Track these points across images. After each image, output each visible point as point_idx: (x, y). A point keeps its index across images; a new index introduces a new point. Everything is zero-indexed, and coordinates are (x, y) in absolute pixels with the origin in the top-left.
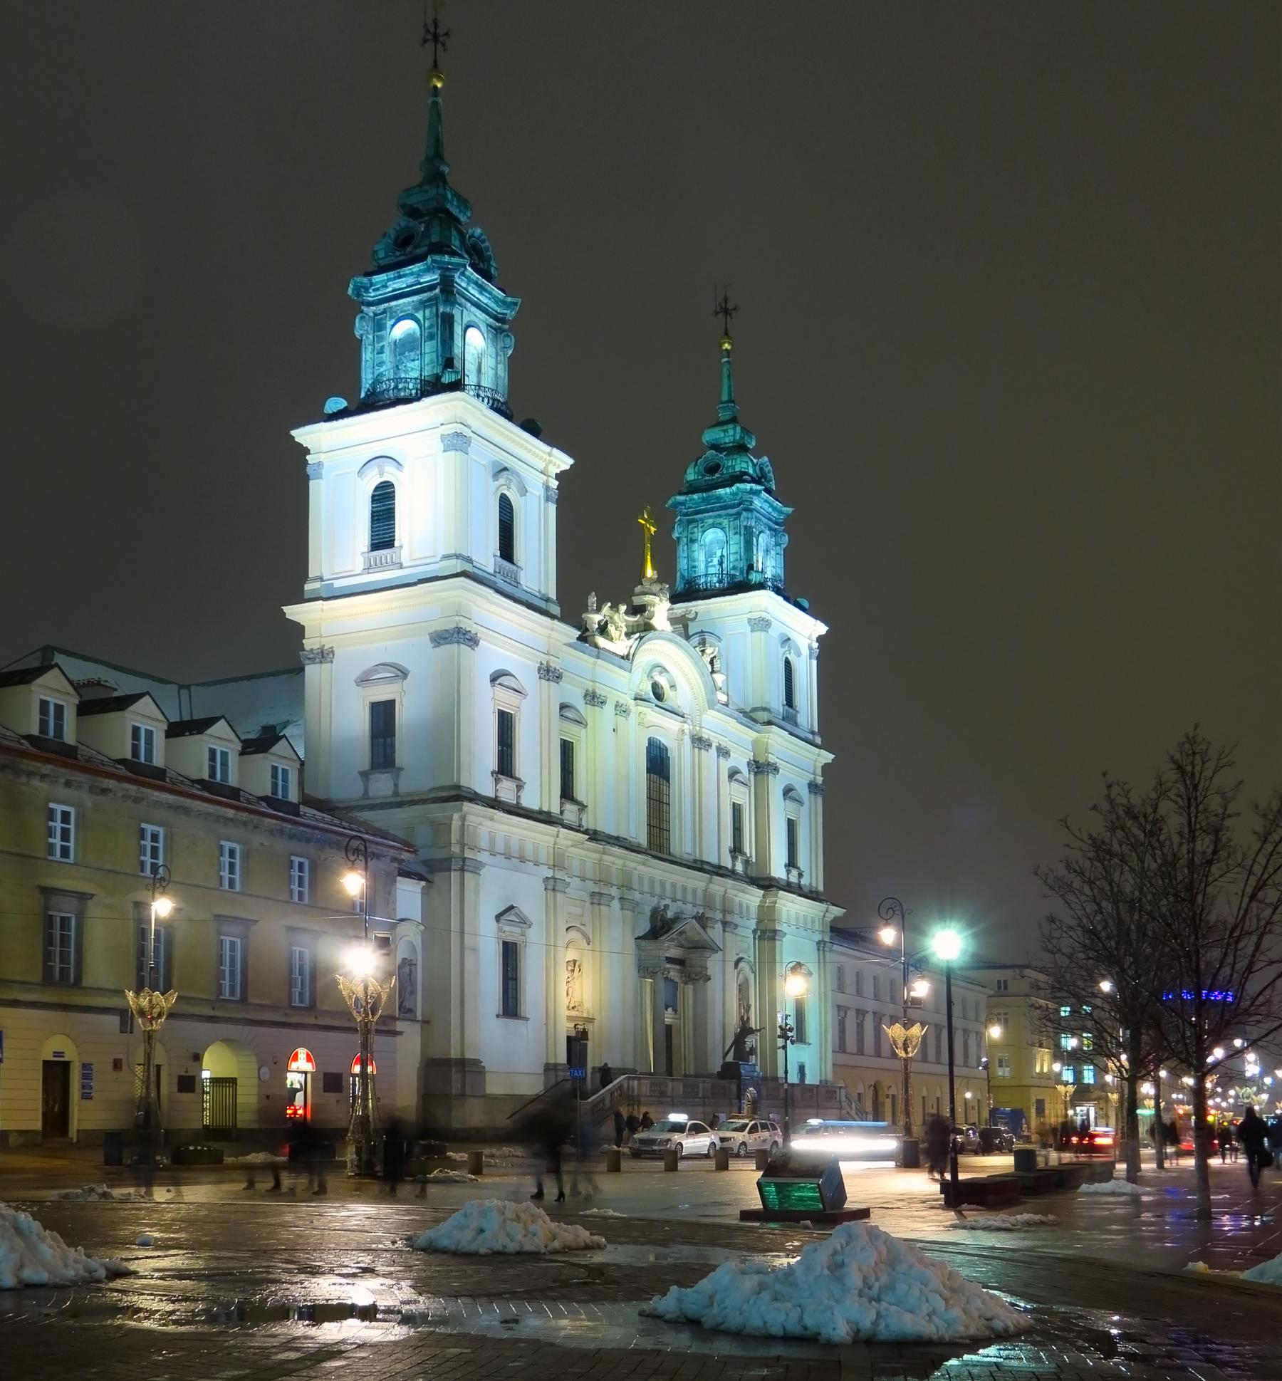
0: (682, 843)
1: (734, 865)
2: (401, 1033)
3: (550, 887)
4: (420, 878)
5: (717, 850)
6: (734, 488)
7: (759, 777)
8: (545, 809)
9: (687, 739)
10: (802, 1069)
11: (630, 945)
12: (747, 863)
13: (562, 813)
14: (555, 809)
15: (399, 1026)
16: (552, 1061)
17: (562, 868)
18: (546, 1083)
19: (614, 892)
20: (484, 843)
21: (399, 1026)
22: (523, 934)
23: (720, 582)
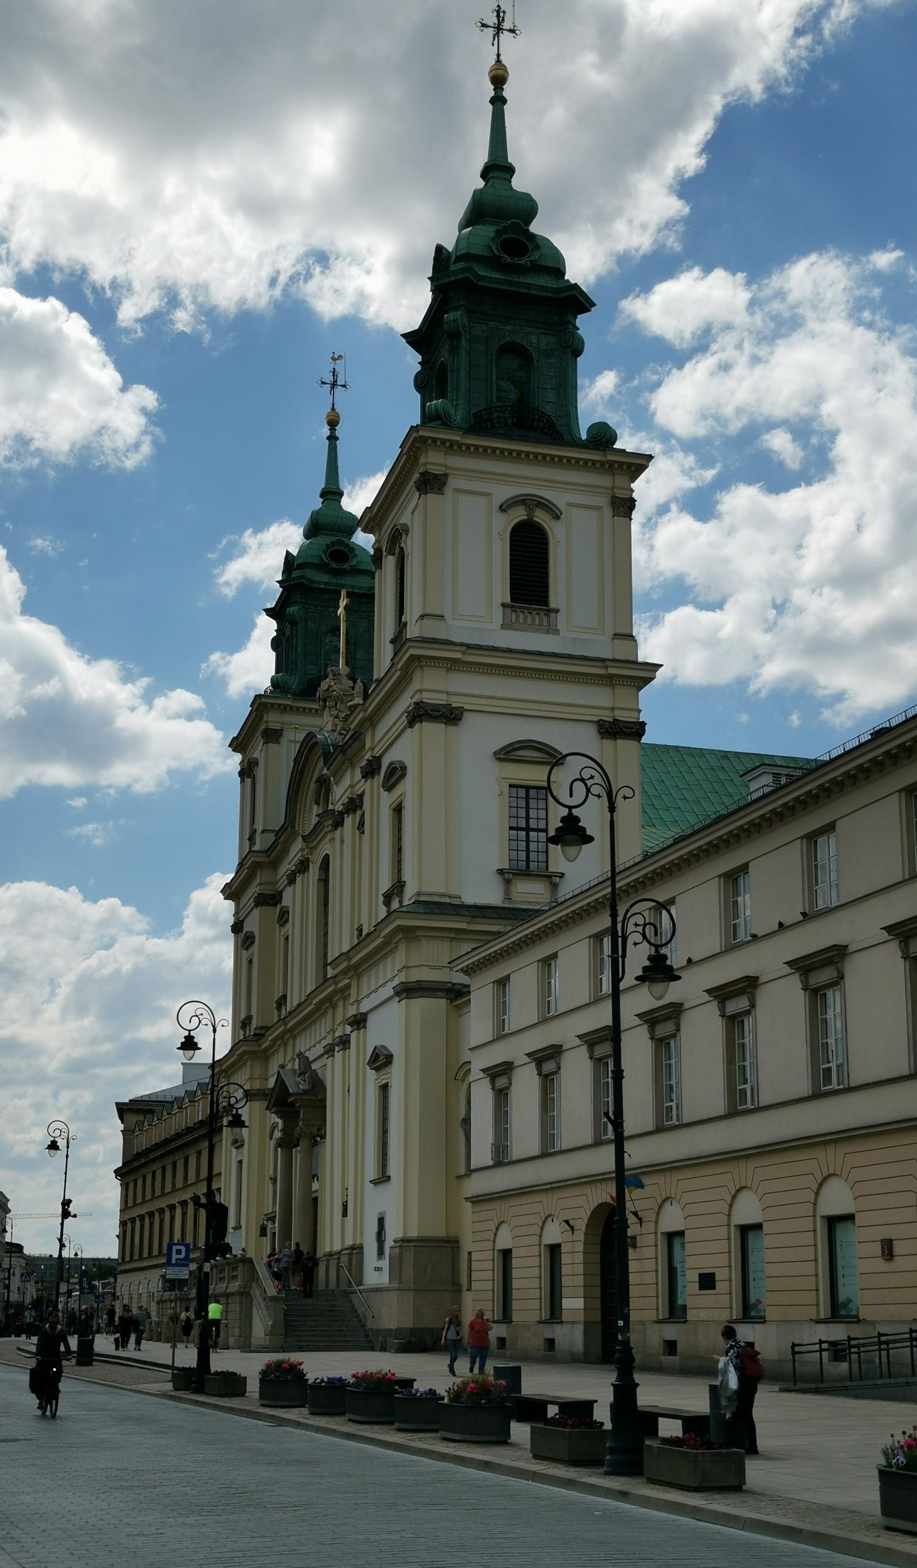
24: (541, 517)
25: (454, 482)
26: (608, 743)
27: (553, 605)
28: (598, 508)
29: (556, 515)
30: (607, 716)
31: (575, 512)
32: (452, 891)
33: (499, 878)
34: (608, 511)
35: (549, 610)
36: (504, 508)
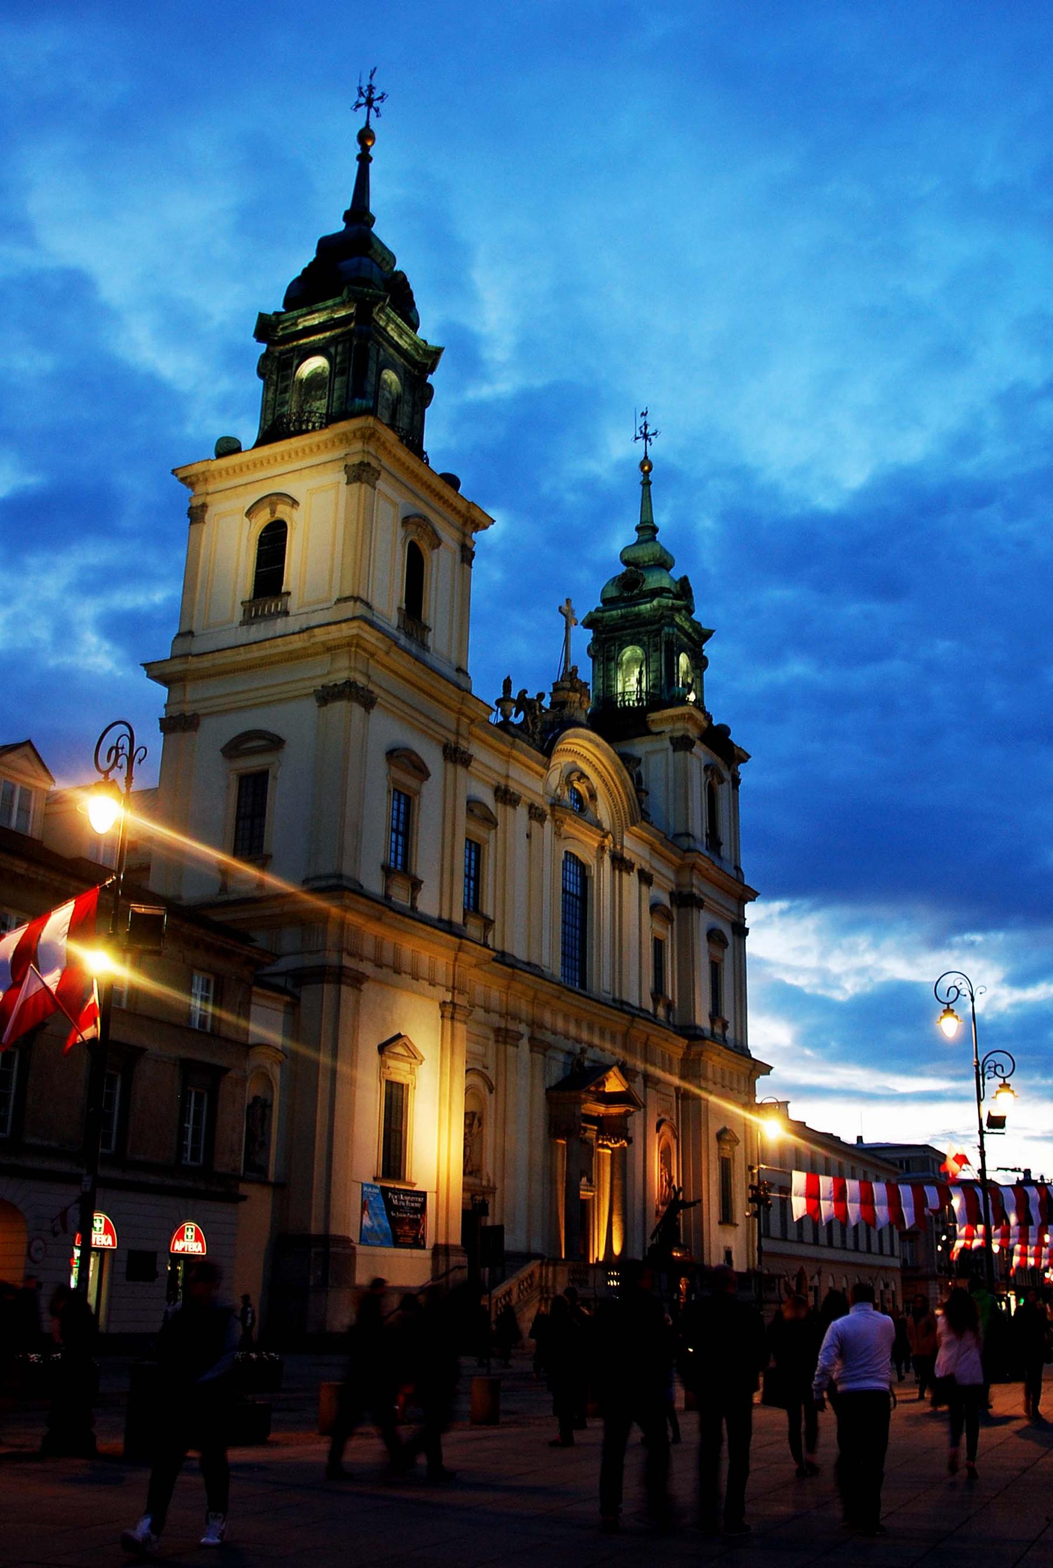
0: (601, 980)
1: (655, 1009)
2: (244, 1198)
3: (448, 1014)
4: (282, 991)
5: (637, 991)
6: (655, 603)
7: (681, 910)
8: (445, 917)
9: (607, 858)
10: (728, 1254)
11: (540, 1093)
12: (669, 1007)
13: (465, 924)
14: (458, 918)
15: (244, 1189)
16: (442, 1241)
17: (462, 992)
18: (435, 1268)
19: (523, 1028)
20: (368, 949)
21: (244, 1189)
22: (412, 1072)
23: (639, 700)
25: (380, 484)
26: (450, 766)
34: (458, 556)
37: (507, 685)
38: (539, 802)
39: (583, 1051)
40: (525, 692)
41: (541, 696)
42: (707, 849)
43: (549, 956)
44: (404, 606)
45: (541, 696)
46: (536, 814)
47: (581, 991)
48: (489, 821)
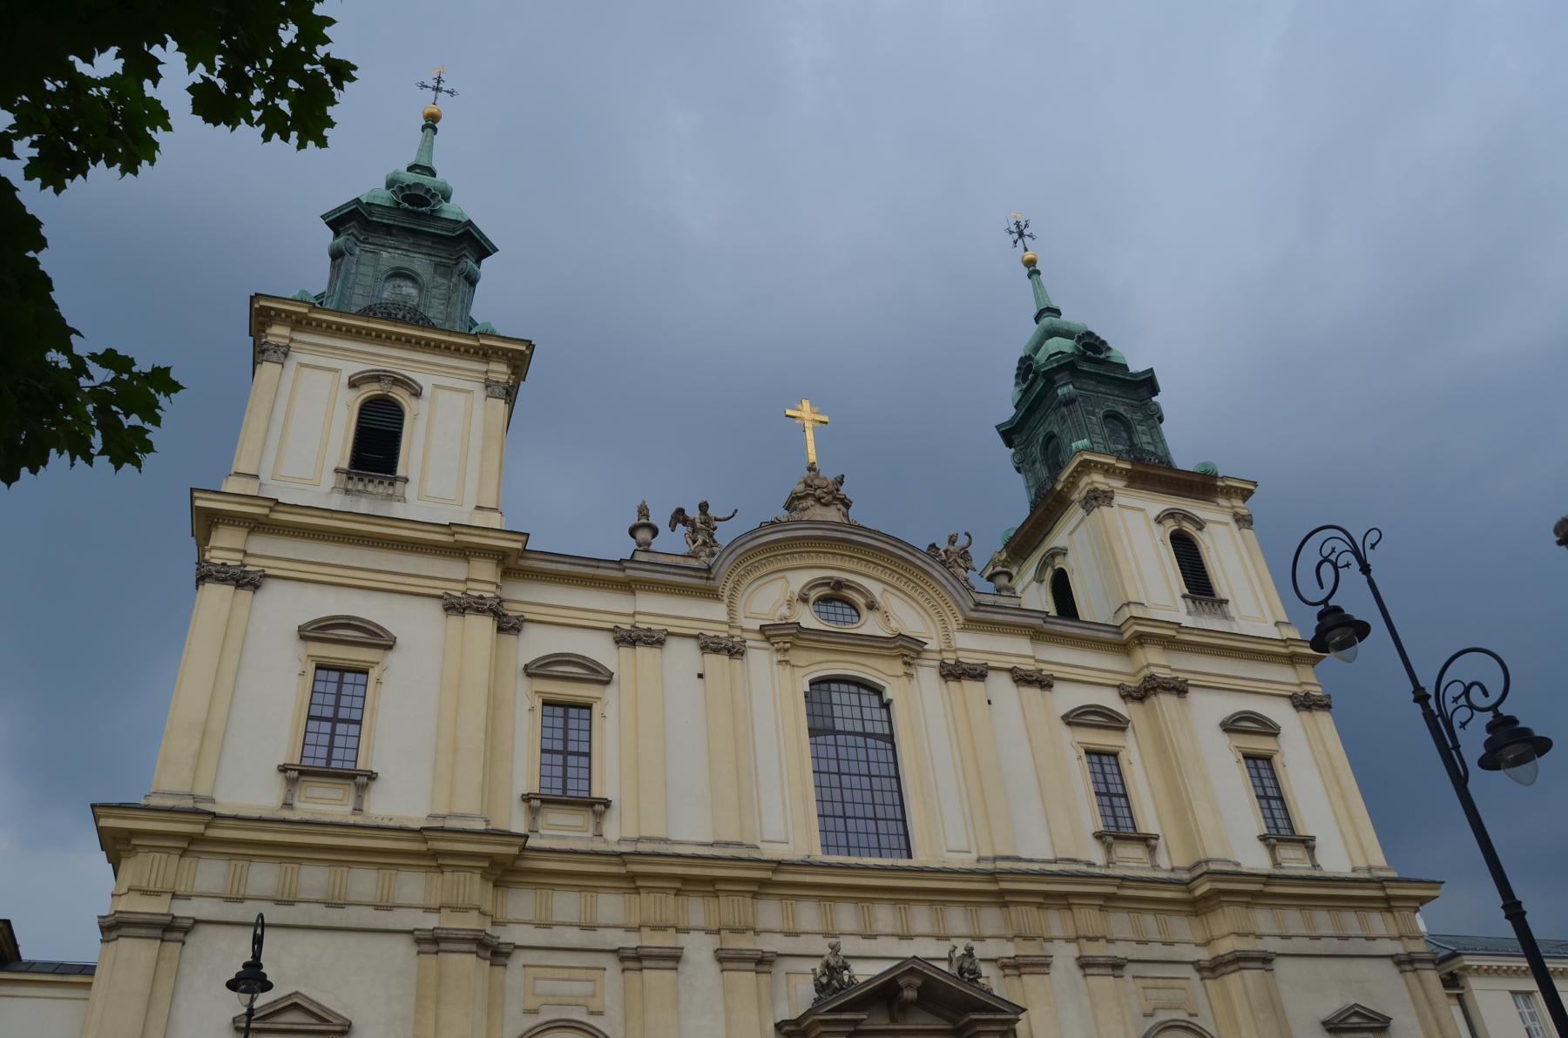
7: (1147, 702)
24: (399, 395)
25: (297, 357)
26: (455, 620)
27: (400, 472)
28: (469, 392)
29: (417, 394)
30: (456, 590)
31: (442, 394)
32: (201, 791)
33: (279, 779)
35: (396, 479)
36: (353, 384)
37: (643, 511)
38: (722, 631)
39: (835, 949)
40: (680, 511)
41: (703, 507)
42: (1189, 613)
43: (788, 826)
44: (345, 465)
45: (703, 507)
46: (710, 646)
47: (904, 862)
48: (600, 676)
